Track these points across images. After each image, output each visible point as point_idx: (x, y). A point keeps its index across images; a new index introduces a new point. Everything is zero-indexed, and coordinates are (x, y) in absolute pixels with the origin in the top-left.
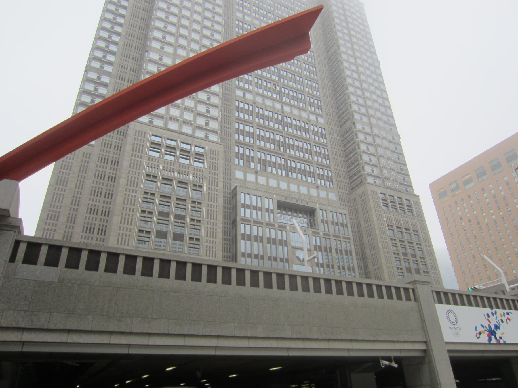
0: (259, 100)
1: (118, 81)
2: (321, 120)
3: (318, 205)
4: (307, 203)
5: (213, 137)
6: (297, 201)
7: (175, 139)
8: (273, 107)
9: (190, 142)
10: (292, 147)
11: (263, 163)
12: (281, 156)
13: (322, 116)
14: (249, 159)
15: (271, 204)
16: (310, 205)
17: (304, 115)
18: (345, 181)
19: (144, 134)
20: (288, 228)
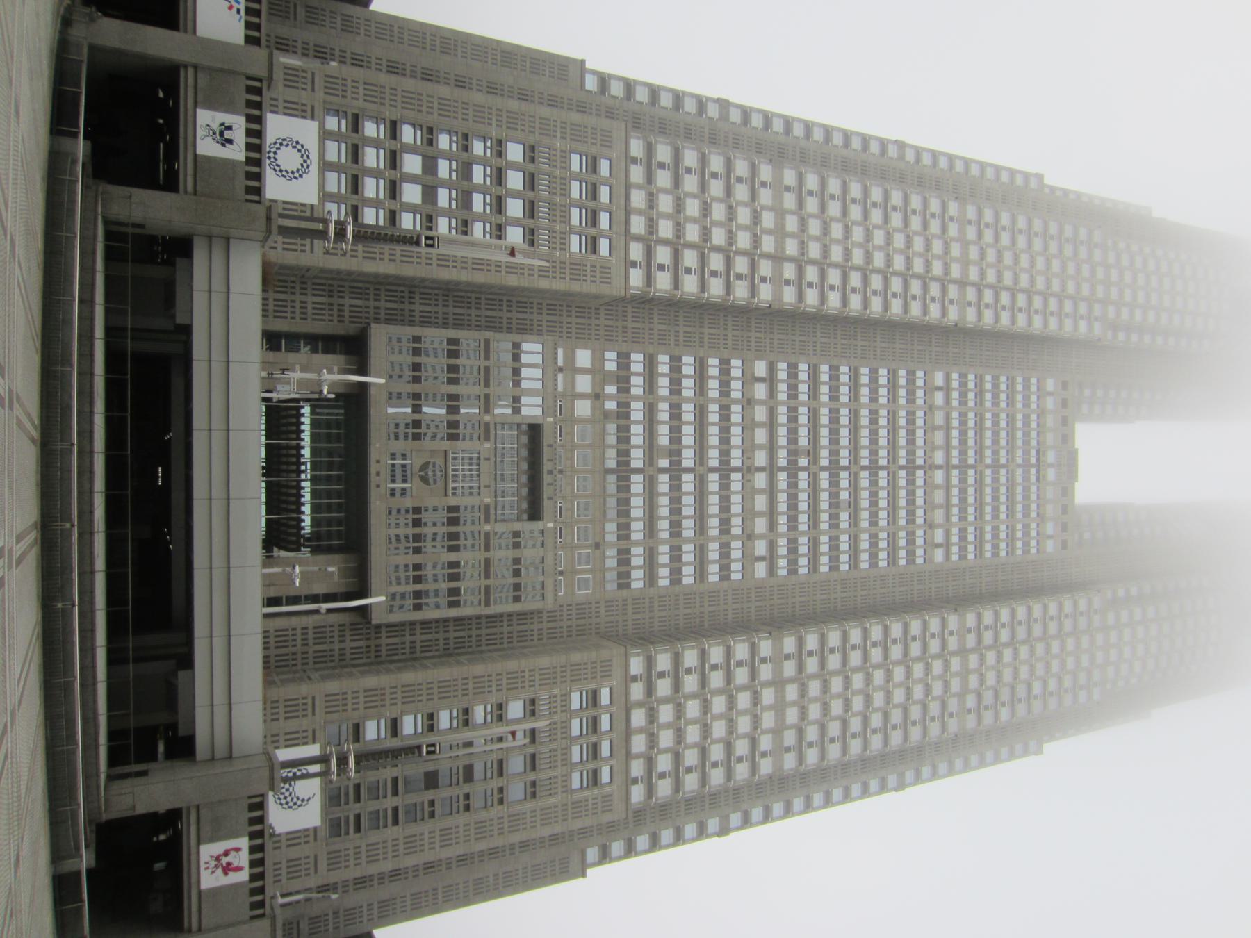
0: (760, 414)
1: (706, 130)
2: (761, 570)
3: (550, 525)
4: (550, 499)
5: (636, 278)
6: (550, 472)
7: (614, 200)
8: (754, 447)
9: (614, 227)
10: (676, 487)
11: (623, 414)
12: (650, 458)
13: (772, 570)
14: (623, 381)
15: (532, 409)
16: (547, 504)
17: (760, 525)
18: (630, 623)
19: (607, 143)
20: (487, 445)
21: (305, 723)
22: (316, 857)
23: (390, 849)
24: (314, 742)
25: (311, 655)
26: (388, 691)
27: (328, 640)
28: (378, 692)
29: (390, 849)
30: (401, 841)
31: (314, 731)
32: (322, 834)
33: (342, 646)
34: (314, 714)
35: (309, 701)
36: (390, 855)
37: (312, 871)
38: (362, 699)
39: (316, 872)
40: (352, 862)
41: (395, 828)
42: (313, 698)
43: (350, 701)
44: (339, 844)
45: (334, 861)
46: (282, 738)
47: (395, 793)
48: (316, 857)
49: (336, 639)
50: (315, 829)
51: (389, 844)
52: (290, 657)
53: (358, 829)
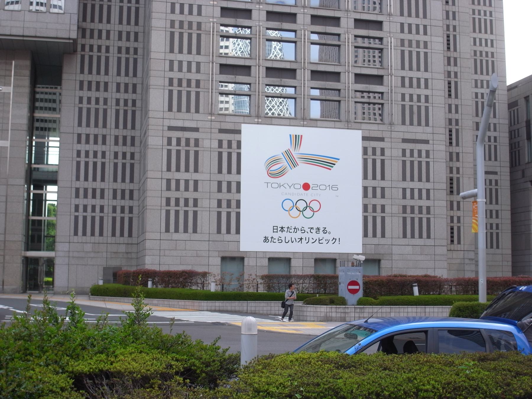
21: (209, 143)
22: (405, 141)
23: (414, 37)
24: (239, 132)
25: (121, 132)
26: (177, 17)
27: (101, 106)
28: (177, 31)
29: (414, 37)
30: (406, 20)
31: (221, 131)
32: (375, 130)
33: (112, 87)
34: (196, 130)
35: (175, 134)
36: (422, 38)
37: (424, 147)
38: (185, 57)
39: (426, 142)
40: (423, 92)
41: (385, 26)
42: (171, 128)
43: (185, 75)
44: (393, 109)
45: (416, 115)
46: (225, 177)
47: (336, 21)
48: (405, 141)
49: (102, 95)
50: (364, 138)
51: (406, 36)
52: (120, 161)
53: (379, 79)
